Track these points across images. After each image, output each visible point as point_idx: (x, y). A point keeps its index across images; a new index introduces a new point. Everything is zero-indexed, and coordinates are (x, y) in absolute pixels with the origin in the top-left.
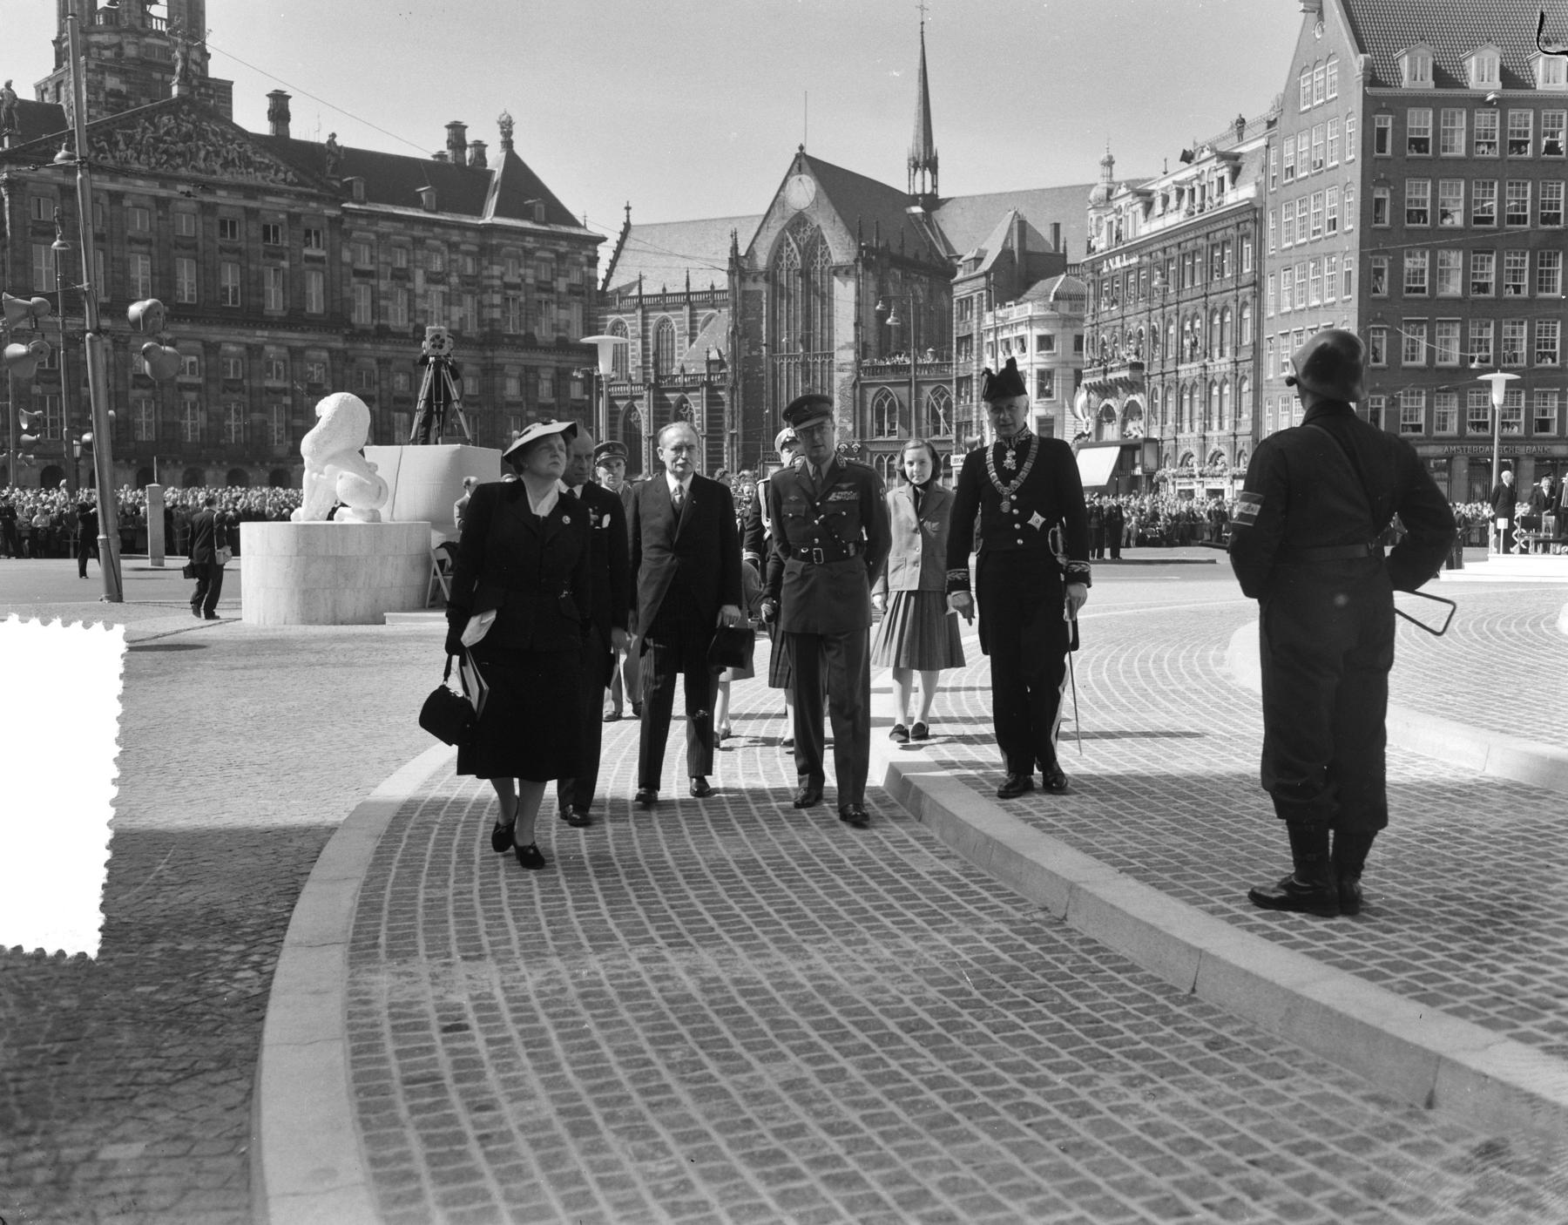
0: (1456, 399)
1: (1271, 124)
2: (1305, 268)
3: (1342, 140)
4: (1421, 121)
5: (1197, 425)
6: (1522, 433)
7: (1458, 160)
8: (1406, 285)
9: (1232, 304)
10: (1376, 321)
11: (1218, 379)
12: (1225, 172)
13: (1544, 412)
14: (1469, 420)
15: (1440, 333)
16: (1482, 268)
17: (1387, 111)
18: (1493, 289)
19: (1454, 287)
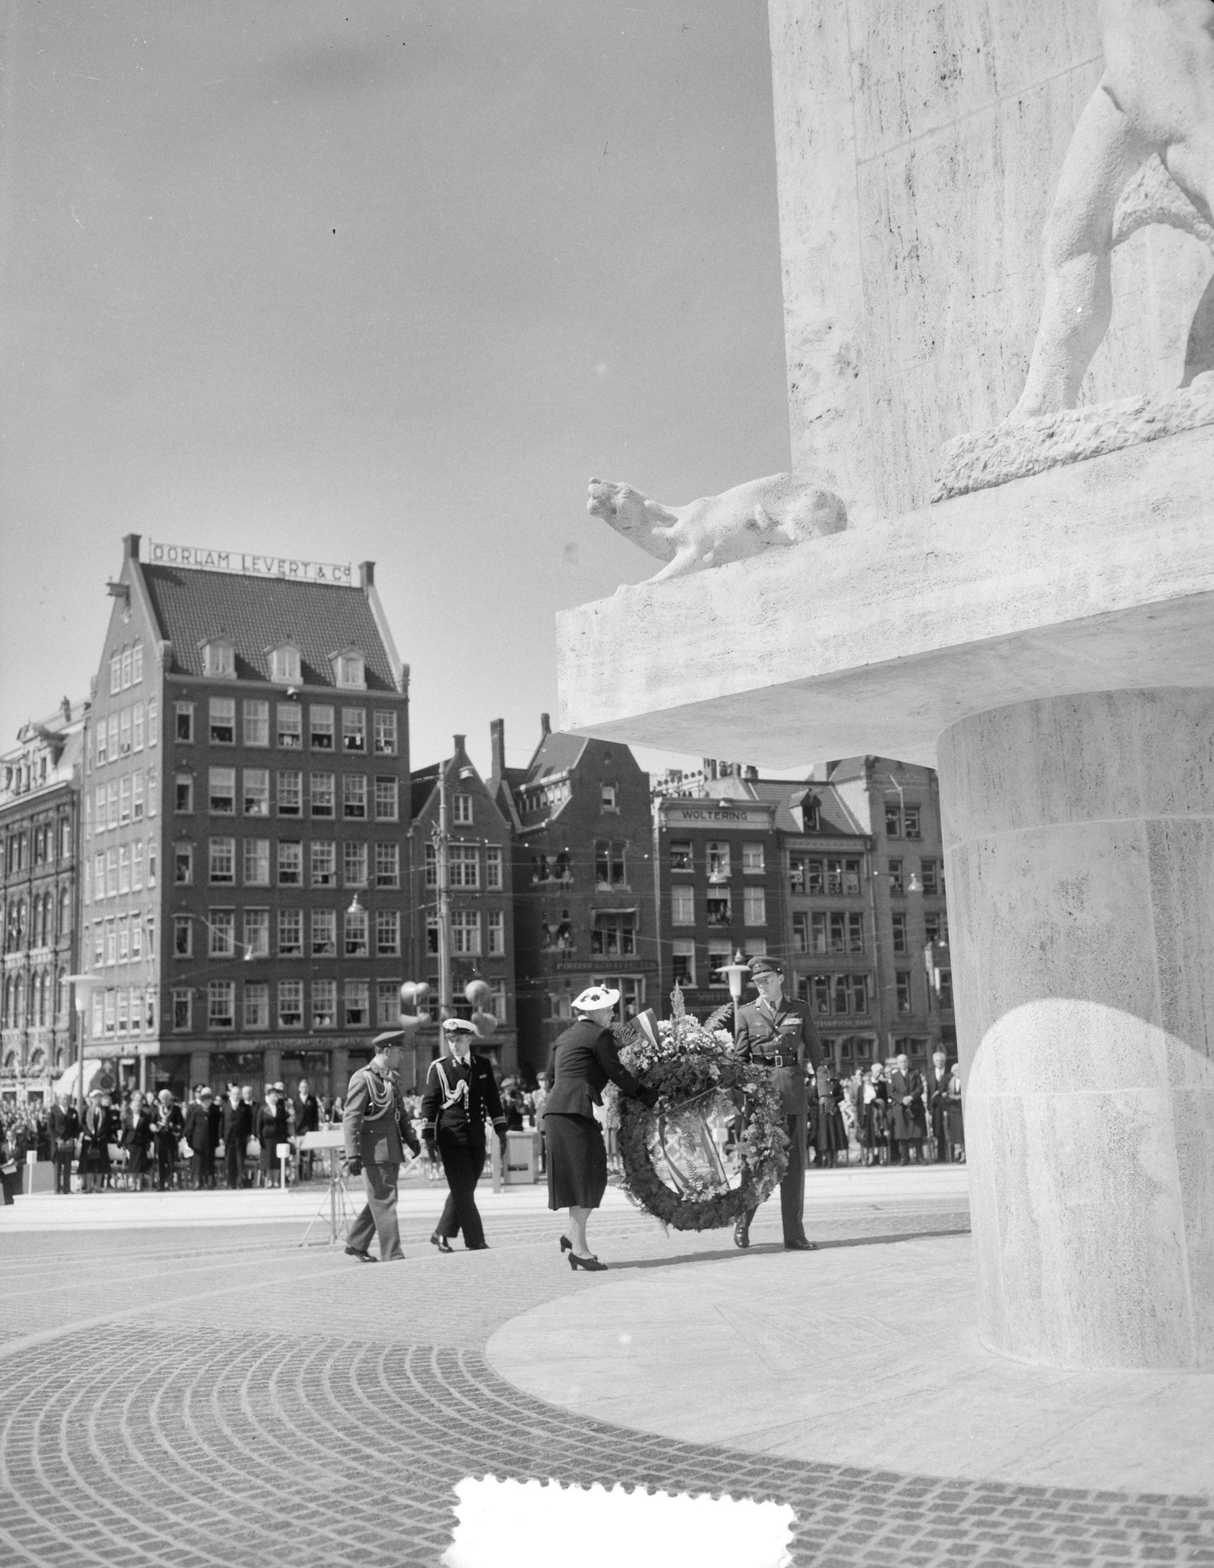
0: (266, 993)
1: (88, 706)
2: (118, 852)
3: (146, 725)
4: (222, 711)
5: (21, 1021)
6: (334, 1026)
7: (260, 750)
8: (211, 873)
9: (52, 890)
10: (181, 909)
11: (40, 969)
12: (47, 753)
13: (356, 1002)
14: (280, 1012)
15: (248, 923)
16: (355, 854)
17: (189, 698)
18: (301, 878)
19: (262, 875)
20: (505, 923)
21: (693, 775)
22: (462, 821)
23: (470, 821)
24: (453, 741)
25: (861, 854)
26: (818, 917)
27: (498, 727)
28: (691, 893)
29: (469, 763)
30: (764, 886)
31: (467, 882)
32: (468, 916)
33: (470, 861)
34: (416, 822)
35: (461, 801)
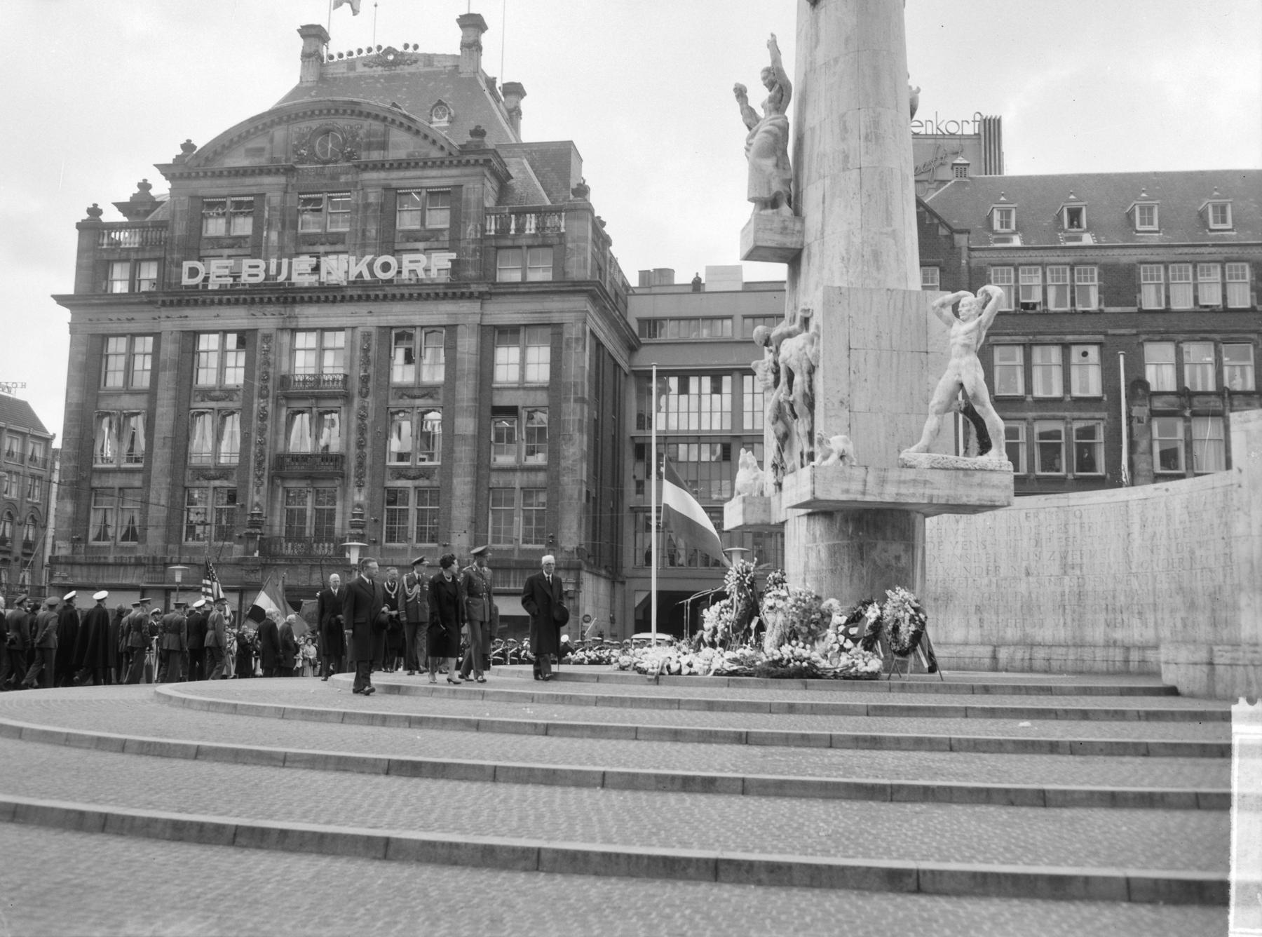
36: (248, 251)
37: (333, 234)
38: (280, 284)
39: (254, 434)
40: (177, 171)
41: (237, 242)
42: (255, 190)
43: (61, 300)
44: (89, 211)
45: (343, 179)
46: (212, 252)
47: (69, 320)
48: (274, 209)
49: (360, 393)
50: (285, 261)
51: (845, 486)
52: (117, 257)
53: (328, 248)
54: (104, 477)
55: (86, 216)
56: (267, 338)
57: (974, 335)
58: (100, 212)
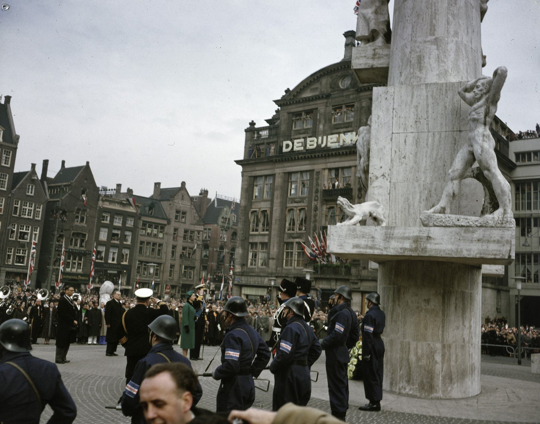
20: (39, 232)
21: (112, 190)
22: (30, 194)
23: (33, 194)
24: (31, 165)
25: (165, 225)
26: (148, 243)
27: (46, 163)
28: (107, 230)
29: (36, 174)
30: (132, 231)
31: (28, 215)
32: (26, 227)
33: (30, 208)
34: (13, 191)
35: (31, 187)
36: (310, 135)
37: (346, 123)
38: (324, 148)
39: (312, 217)
40: (282, 103)
41: (306, 131)
42: (313, 107)
43: (238, 162)
44: (250, 124)
45: (351, 97)
46: (296, 137)
47: (241, 171)
48: (321, 114)
49: (358, 196)
50: (325, 137)
51: (356, 241)
52: (259, 142)
53: (345, 130)
54: (254, 237)
55: (249, 126)
56: (318, 173)
57: (482, 110)
58: (255, 124)
